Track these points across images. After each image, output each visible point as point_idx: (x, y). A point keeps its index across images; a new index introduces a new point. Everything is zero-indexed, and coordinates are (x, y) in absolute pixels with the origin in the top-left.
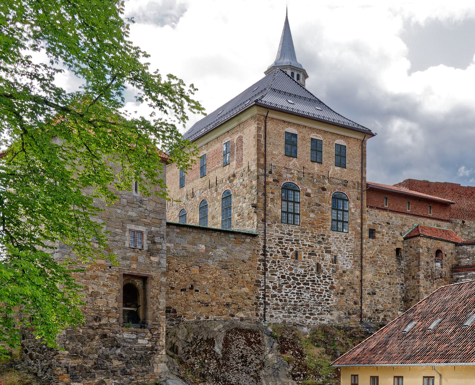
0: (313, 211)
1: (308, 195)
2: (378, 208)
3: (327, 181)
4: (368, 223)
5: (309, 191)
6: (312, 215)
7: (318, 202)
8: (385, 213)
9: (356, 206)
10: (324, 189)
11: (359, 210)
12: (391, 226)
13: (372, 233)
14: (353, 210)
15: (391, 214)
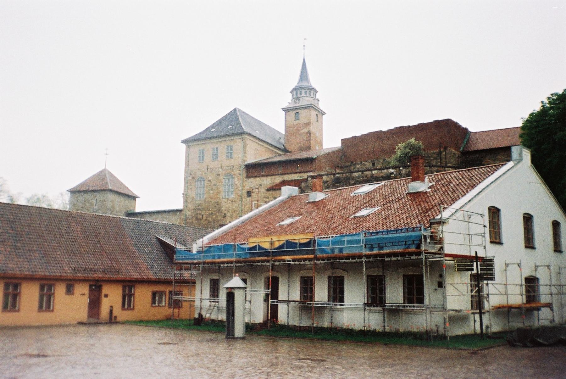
0: (212, 189)
1: (210, 181)
2: (252, 177)
3: (220, 170)
4: (247, 188)
5: (210, 178)
6: (211, 192)
7: (215, 184)
8: (258, 179)
9: (239, 180)
10: (219, 175)
11: (240, 182)
12: (263, 186)
13: (249, 194)
14: (236, 183)
15: (263, 178)
